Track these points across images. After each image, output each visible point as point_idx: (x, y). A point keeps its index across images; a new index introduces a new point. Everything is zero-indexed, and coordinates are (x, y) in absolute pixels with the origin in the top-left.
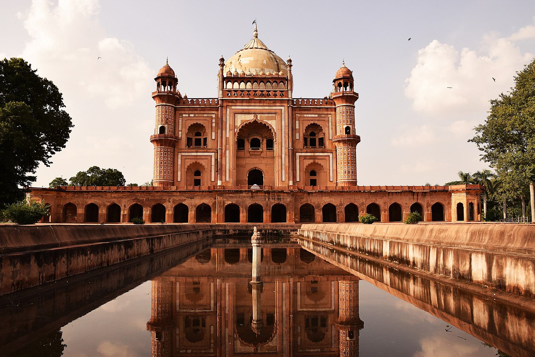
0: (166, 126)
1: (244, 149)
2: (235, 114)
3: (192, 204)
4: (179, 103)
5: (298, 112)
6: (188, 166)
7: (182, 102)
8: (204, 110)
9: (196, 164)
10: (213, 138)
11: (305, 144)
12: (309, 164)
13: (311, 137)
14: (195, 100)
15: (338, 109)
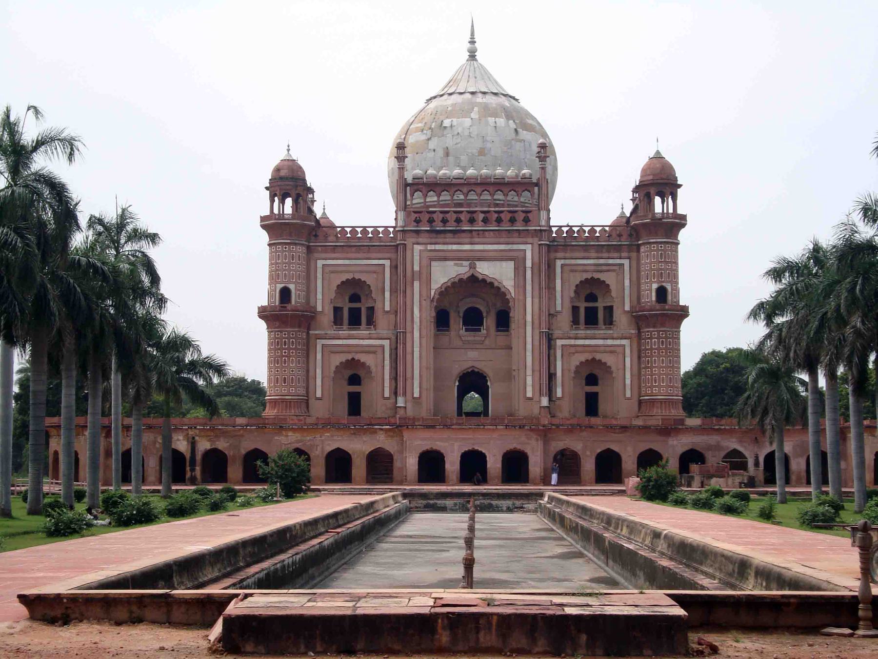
0: (292, 287)
1: (448, 331)
2: (432, 259)
3: (359, 447)
4: (316, 236)
5: (560, 255)
6: (337, 367)
7: (320, 233)
8: (369, 252)
9: (352, 363)
10: (387, 308)
11: (575, 321)
12: (581, 363)
13: (591, 305)
14: (348, 230)
15: (642, 249)
